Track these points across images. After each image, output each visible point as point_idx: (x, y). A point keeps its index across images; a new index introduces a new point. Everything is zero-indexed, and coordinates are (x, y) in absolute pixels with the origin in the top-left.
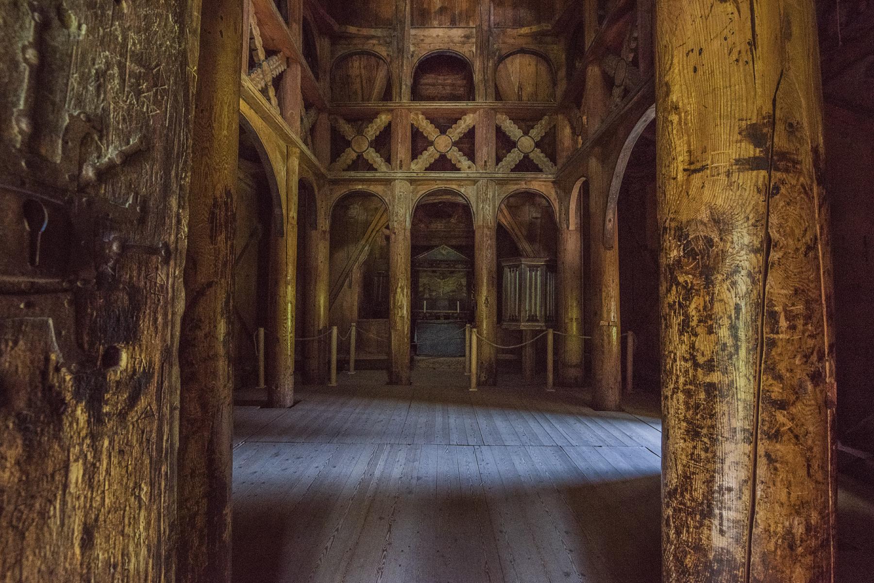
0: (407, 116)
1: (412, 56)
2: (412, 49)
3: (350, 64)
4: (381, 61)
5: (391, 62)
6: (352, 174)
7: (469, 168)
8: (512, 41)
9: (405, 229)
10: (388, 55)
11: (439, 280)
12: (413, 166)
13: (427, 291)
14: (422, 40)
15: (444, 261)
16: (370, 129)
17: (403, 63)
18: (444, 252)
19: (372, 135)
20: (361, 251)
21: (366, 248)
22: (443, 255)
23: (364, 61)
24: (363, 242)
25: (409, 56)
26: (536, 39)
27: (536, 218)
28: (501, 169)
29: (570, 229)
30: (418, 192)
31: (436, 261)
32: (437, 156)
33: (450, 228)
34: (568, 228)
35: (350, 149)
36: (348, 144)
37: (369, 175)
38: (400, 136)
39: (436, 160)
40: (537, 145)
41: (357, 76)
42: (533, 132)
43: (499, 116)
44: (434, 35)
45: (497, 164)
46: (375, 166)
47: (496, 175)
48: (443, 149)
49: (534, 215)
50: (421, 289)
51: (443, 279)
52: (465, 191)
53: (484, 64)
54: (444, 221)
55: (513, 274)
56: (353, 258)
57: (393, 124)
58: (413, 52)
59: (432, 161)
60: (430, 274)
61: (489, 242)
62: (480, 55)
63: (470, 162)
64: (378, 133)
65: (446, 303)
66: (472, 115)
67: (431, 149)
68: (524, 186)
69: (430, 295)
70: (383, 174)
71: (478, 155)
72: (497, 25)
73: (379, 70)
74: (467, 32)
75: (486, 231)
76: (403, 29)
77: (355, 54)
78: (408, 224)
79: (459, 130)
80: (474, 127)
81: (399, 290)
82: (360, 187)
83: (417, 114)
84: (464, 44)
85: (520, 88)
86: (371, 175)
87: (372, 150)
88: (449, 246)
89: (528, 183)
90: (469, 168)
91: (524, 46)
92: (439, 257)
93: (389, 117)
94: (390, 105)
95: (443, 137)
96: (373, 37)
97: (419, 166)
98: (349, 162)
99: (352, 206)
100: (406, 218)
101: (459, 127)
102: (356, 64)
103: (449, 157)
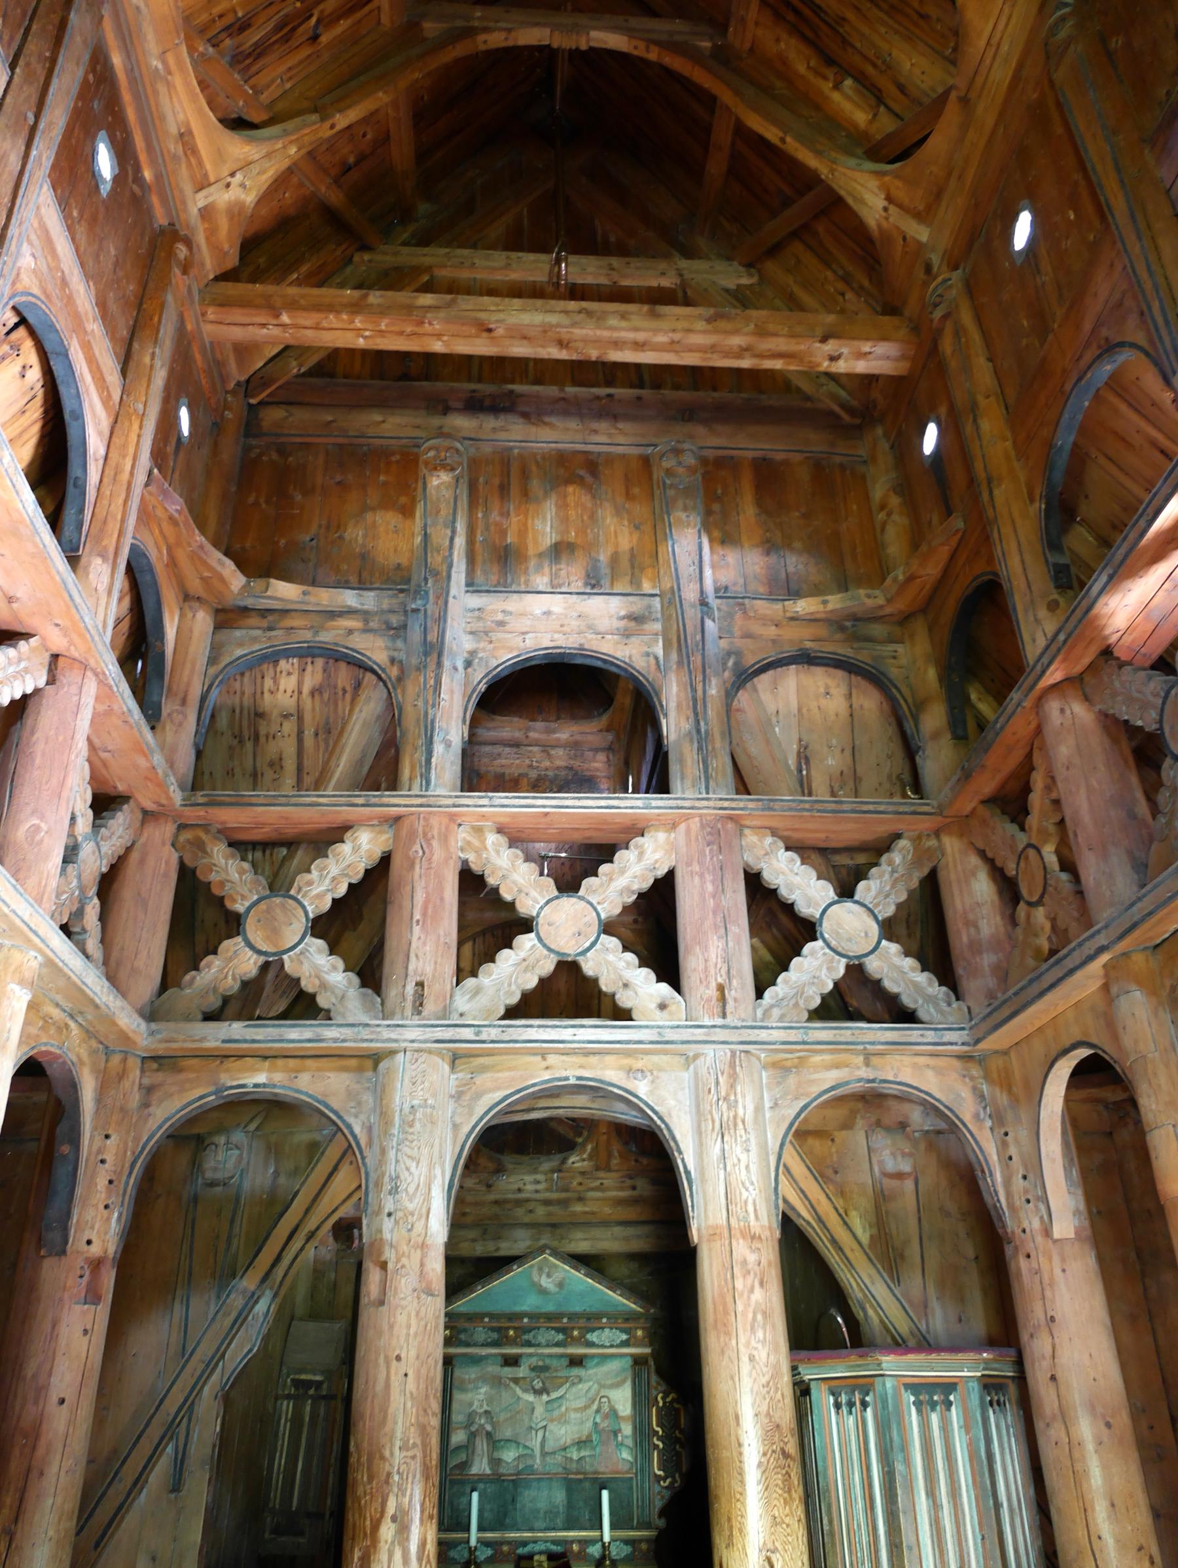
0: (445, 839)
1: (468, 664)
2: (468, 643)
3: (268, 683)
4: (369, 677)
5: (400, 679)
6: (237, 1029)
7: (662, 1007)
8: (772, 631)
9: (423, 1246)
10: (392, 661)
11: (530, 1397)
12: (462, 1002)
13: (481, 1445)
14: (501, 624)
15: (550, 1317)
16: (315, 874)
17: (438, 682)
18: (545, 1282)
19: (320, 896)
20: (240, 1320)
21: (261, 1307)
22: (543, 1292)
23: (314, 675)
24: (248, 1282)
25: (460, 665)
26: (842, 629)
27: (899, 1176)
28: (776, 1012)
29: (1057, 1234)
30: (478, 1096)
32: (547, 966)
33: (566, 1189)
34: (1047, 1232)
35: (239, 939)
36: (233, 924)
37: (297, 1033)
38: (420, 897)
39: (542, 981)
40: (888, 929)
41: (286, 716)
42: (865, 890)
43: (751, 838)
44: (538, 612)
45: (759, 994)
46: (322, 1001)
47: (763, 1035)
48: (570, 947)
49: (890, 1166)
52: (651, 1092)
53: (694, 690)
54: (546, 1166)
55: (851, 1420)
56: (205, 1350)
57: (396, 863)
58: (473, 653)
59: (532, 983)
60: (494, 1369)
61: (758, 1295)
62: (680, 663)
63: (665, 988)
64: (342, 890)
65: (559, 1496)
66: (661, 836)
67: (525, 942)
68: (864, 1073)
70: (347, 1032)
71: (692, 963)
72: (722, 592)
73: (363, 696)
74: (636, 605)
75: (741, 1248)
76: (443, 596)
77: (288, 654)
78: (437, 1228)
79: (621, 882)
80: (671, 874)
81: (387, 1531)
82: (261, 1078)
83: (479, 830)
84: (628, 636)
85: (804, 757)
86: (308, 1034)
87: (317, 945)
89: (875, 1060)
90: (662, 1007)
91: (809, 645)
92: (530, 1303)
93: (384, 837)
94: (394, 802)
95: (569, 904)
96: (350, 612)
97: (483, 1001)
98: (231, 985)
99: (222, 1140)
100: (428, 1197)
101: (622, 871)
102: (288, 683)
103: (589, 967)
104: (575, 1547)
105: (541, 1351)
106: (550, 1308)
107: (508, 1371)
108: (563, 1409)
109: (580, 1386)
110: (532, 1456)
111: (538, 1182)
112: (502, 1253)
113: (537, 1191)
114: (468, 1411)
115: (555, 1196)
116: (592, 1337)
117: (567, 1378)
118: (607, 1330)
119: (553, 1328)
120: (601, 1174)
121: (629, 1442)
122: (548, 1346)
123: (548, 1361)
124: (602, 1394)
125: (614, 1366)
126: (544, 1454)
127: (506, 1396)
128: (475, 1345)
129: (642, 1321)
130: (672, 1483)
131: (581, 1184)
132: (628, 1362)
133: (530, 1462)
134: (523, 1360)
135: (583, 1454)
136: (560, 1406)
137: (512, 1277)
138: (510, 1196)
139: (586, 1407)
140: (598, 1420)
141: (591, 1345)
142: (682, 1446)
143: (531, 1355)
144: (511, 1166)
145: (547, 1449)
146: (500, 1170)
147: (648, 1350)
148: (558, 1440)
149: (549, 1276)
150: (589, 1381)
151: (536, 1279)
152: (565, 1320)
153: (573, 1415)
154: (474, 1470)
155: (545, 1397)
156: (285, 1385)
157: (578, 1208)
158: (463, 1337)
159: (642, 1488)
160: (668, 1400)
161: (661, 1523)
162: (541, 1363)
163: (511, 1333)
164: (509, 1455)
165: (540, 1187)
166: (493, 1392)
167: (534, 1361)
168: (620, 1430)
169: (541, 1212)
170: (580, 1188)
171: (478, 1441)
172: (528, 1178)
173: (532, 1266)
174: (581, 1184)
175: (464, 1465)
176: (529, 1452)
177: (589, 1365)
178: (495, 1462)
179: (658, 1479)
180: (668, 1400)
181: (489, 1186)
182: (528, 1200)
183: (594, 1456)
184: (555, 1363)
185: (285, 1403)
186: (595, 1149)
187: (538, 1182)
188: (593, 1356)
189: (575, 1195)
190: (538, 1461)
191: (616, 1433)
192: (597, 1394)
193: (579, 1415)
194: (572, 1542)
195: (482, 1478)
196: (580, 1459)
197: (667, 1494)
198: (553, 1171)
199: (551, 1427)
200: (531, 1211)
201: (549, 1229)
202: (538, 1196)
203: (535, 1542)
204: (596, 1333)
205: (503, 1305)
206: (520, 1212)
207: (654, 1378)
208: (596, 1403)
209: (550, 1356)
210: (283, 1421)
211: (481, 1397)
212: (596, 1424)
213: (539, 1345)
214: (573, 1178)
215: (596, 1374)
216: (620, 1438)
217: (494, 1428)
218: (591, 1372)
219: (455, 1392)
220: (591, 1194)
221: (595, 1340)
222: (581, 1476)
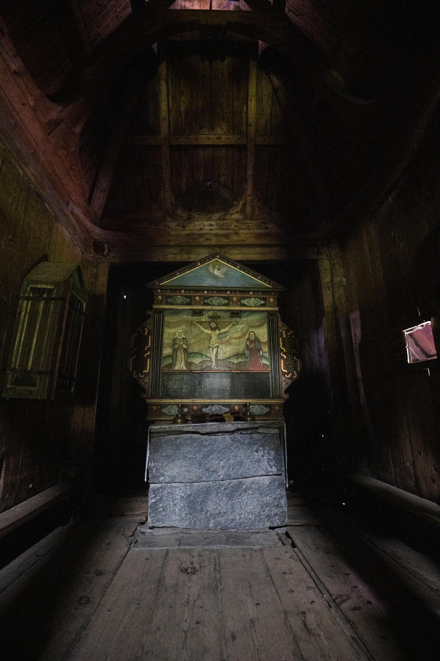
11: (209, 332)
13: (181, 355)
15: (220, 290)
18: (216, 272)
22: (216, 277)
31: (199, 290)
50: (167, 351)
51: (217, 328)
54: (216, 216)
65: (226, 382)
69: (189, 364)
88: (228, 261)
92: (208, 282)
104: (236, 408)
105: (214, 308)
106: (220, 285)
107: (196, 318)
108: (228, 337)
109: (238, 326)
110: (212, 362)
111: (211, 225)
112: (192, 260)
113: (211, 230)
114: (172, 337)
115: (221, 232)
116: (245, 302)
117: (230, 322)
118: (253, 299)
119: (222, 297)
120: (248, 221)
121: (267, 355)
122: (219, 305)
123: (219, 314)
124: (250, 330)
125: (257, 317)
126: (217, 360)
127: (195, 331)
128: (176, 304)
129: (273, 294)
130: (292, 376)
131: (236, 226)
132: (265, 314)
133: (209, 364)
134: (205, 313)
135: (240, 360)
136: (226, 337)
137: (196, 270)
138: (197, 232)
139: (240, 338)
140: (248, 343)
141: (244, 305)
143: (209, 310)
144: (196, 216)
145: (219, 358)
146: (190, 219)
147: (277, 309)
148: (225, 353)
149: (219, 269)
150: (242, 324)
151: (211, 271)
152: (228, 293)
153: (234, 341)
154: (177, 368)
155: (217, 332)
156: (25, 292)
157: (235, 238)
158: (169, 300)
159: (275, 380)
161: (286, 396)
163: (197, 298)
164: (197, 361)
165: (212, 227)
166: (187, 328)
167: (210, 313)
168: (261, 349)
169: (214, 241)
170: (235, 228)
171: (179, 353)
172: (206, 223)
173: (209, 264)
174: (236, 226)
175: (171, 365)
176: (209, 359)
177: (242, 316)
178: (189, 364)
179: (284, 374)
180: (288, 334)
181: (184, 227)
182: (206, 234)
183: (246, 362)
184: (223, 314)
185: (25, 302)
186: (244, 205)
187: (211, 225)
188: (245, 311)
189: (233, 232)
190: (214, 364)
191: (259, 350)
192: (248, 330)
193: (237, 341)
194: (234, 405)
195: (181, 372)
196: (238, 363)
197: (290, 382)
198: (219, 219)
199: (221, 346)
200: (208, 239)
201: (219, 249)
202: (212, 232)
203: (213, 405)
204: (247, 300)
205: (193, 283)
206: (201, 240)
207: (280, 324)
208: (248, 335)
209: (220, 311)
210: (23, 313)
211: (180, 331)
212: (247, 346)
213: (214, 305)
214: (232, 223)
215: (247, 320)
216: (261, 353)
217: (187, 346)
218: (244, 319)
219: (165, 328)
220: (241, 231)
221: (246, 303)
222: (240, 372)
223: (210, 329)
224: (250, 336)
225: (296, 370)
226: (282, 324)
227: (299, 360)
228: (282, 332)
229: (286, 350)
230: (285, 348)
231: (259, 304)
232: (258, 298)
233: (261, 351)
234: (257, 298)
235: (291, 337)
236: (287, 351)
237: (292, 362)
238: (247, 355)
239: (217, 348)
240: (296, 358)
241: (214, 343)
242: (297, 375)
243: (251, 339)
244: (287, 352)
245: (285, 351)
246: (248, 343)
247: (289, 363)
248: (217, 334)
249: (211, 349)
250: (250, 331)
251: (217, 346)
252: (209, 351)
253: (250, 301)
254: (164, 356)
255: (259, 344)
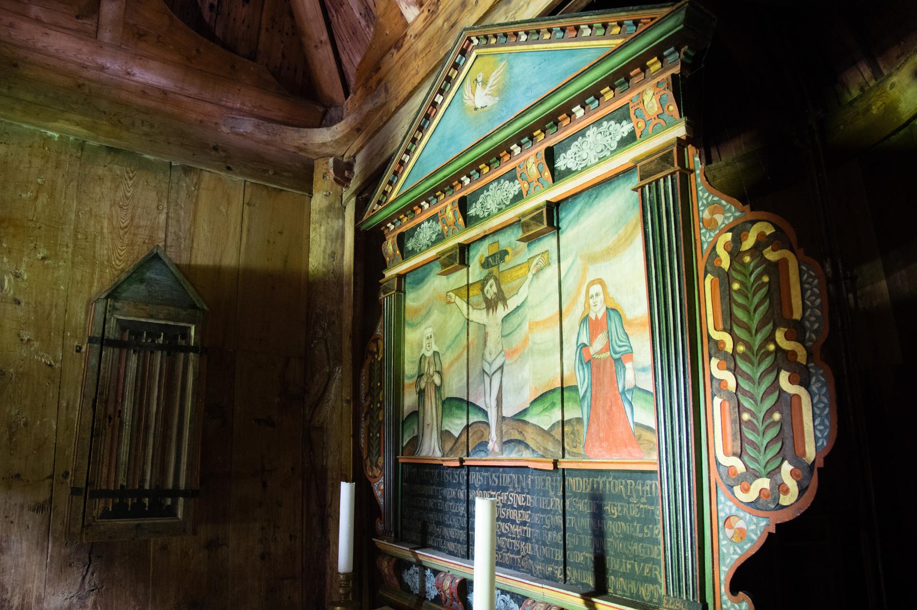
121: (647, 382)
126: (502, 419)
142: (802, 378)
160: (748, 243)
162: (494, 250)
192: (584, 277)
208: (582, 298)
216: (629, 374)
223: (484, 305)
224: (591, 301)
225: (797, 460)
226: (713, 202)
227: (812, 395)
228: (714, 248)
229: (736, 341)
230: (731, 332)
231: (614, 145)
232: (608, 117)
233: (628, 365)
234: (605, 123)
235: (764, 260)
236: (741, 348)
237: (770, 412)
238: (581, 392)
239: (499, 373)
240: (791, 381)
241: (493, 357)
242: (802, 491)
243: (593, 316)
244: (744, 356)
245: (729, 347)
246: (584, 339)
247: (753, 414)
248: (500, 320)
249: (487, 379)
250: (588, 280)
251: (500, 368)
252: (481, 387)
253: (584, 146)
254: (406, 414)
255: (620, 331)
